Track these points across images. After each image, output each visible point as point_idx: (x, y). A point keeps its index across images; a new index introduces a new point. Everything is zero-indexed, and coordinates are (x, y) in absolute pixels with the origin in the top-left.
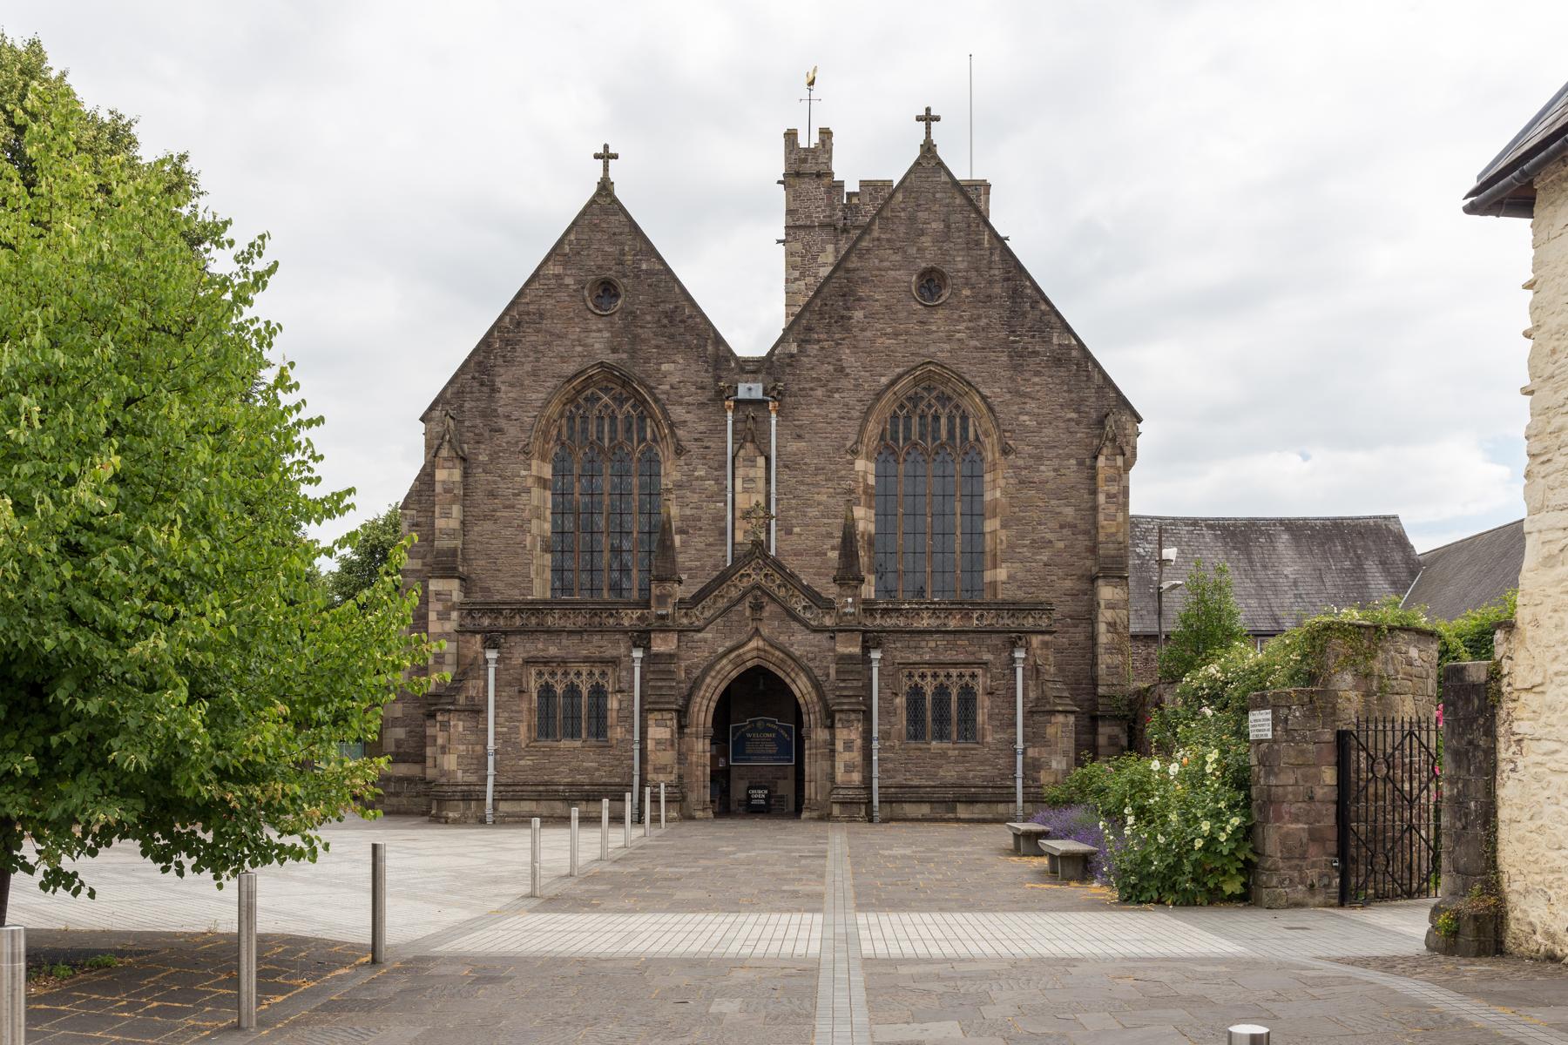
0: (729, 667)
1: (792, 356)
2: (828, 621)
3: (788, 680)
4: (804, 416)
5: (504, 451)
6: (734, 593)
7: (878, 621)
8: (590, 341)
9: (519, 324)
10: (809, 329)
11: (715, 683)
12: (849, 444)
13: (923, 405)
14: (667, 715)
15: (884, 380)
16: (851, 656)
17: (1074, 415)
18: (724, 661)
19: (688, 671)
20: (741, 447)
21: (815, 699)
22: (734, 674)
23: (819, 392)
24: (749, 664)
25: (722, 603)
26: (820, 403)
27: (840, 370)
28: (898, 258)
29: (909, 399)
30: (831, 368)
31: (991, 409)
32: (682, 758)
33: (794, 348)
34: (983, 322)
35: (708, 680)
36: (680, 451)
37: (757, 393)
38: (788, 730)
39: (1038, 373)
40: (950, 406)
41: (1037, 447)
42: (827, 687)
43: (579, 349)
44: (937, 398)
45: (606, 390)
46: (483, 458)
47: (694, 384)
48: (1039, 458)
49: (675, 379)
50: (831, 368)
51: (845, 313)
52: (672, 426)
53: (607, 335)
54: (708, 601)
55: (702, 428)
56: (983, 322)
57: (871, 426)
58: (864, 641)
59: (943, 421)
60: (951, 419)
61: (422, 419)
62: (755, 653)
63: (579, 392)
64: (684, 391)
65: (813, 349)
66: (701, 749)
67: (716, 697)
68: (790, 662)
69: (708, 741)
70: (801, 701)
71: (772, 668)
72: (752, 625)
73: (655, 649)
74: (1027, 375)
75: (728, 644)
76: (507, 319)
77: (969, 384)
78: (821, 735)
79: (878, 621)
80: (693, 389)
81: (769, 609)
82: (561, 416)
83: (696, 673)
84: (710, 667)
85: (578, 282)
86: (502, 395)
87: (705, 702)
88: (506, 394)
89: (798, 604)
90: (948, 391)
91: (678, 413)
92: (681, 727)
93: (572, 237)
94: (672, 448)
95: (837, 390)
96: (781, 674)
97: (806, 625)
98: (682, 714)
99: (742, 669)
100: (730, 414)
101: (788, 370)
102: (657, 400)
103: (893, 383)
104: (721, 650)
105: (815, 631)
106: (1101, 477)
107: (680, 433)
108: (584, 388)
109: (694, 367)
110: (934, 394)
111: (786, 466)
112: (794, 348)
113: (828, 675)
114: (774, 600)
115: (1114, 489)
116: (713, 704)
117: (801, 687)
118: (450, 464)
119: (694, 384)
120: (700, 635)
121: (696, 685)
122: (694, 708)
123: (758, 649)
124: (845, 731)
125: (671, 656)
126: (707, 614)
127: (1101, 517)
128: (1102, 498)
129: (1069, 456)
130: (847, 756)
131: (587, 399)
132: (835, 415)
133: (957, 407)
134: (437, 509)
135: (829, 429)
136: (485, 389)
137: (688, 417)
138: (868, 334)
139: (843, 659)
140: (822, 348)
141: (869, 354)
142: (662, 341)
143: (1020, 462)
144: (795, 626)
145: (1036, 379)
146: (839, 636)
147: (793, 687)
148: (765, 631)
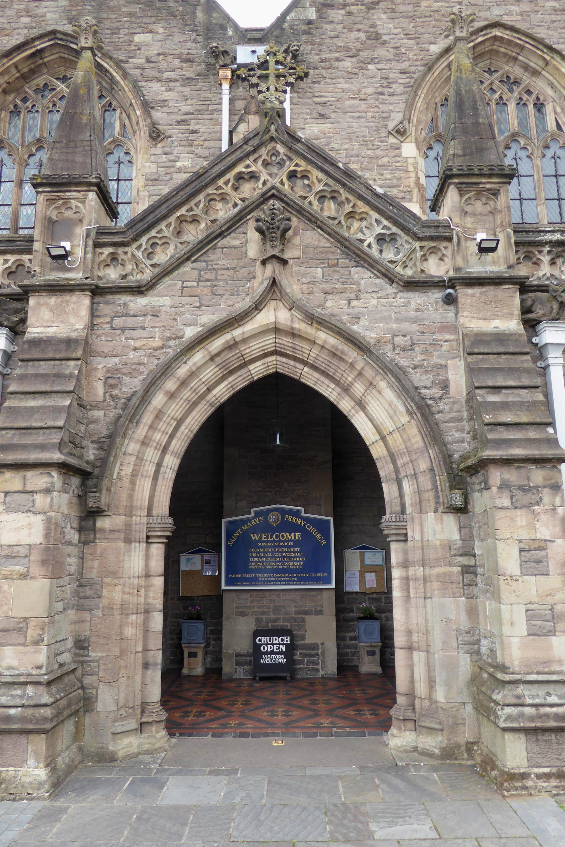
0: (210, 373)
1: (310, 22)
2: (436, 268)
3: (345, 405)
6: (223, 213)
7: (545, 269)
8: (40, 11)
11: (175, 410)
12: (391, 125)
14: (37, 480)
16: (500, 338)
18: (199, 357)
19: (112, 380)
20: (241, 120)
21: (417, 441)
22: (222, 392)
23: (348, 64)
24: (257, 370)
25: (194, 234)
26: (350, 75)
27: (377, 37)
30: (362, 35)
32: (83, 592)
33: (312, 14)
35: (158, 400)
36: (156, 136)
38: (322, 526)
42: (444, 411)
43: (26, 20)
47: (178, 56)
49: (152, 52)
50: (362, 35)
52: (146, 106)
54: (165, 229)
55: (186, 108)
57: (420, 103)
58: (526, 310)
59: (512, 107)
62: (268, 342)
63: (25, 77)
64: (163, 65)
65: (337, 15)
66: (137, 570)
67: (180, 444)
68: (352, 354)
69: (158, 551)
70: (377, 451)
71: (310, 378)
72: (262, 277)
73: (35, 329)
75: (208, 318)
77: (551, 49)
78: (436, 529)
79: (545, 269)
80: (177, 62)
81: (304, 239)
83: (132, 385)
84: (166, 370)
87: (152, 455)
89: (367, 231)
90: (516, 71)
91: (154, 90)
92: (88, 516)
94: (144, 132)
95: (372, 61)
96: (329, 391)
97: (389, 277)
98: (86, 478)
99: (239, 381)
100: (226, 87)
101: (304, 38)
102: (125, 75)
104: (190, 333)
105: (411, 285)
107: (158, 115)
109: (178, 37)
112: (312, 14)
113: (445, 386)
114: (314, 221)
116: (172, 463)
117: (378, 417)
119: (178, 56)
120: (141, 301)
121: (131, 411)
122: (122, 468)
123: (276, 330)
124: (521, 518)
125: (68, 342)
126: (163, 257)
130: (532, 586)
132: (370, 91)
133: (529, 92)
135: (363, 107)
137: (167, 95)
139: (478, 347)
140: (350, 14)
141: (413, 18)
144: (363, 277)
146: (466, 295)
147: (360, 422)
148: (293, 286)
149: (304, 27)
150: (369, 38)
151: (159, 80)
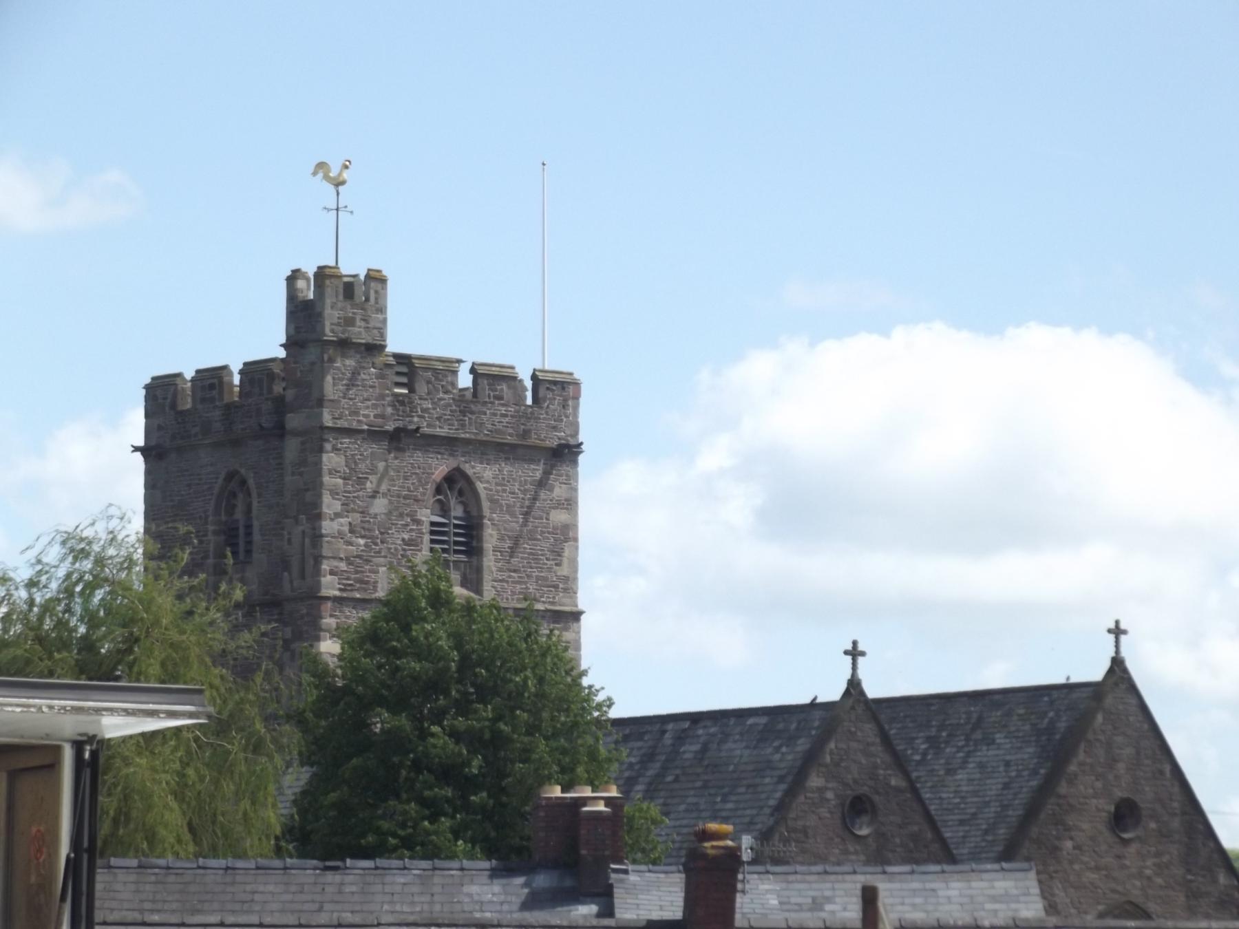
28: (1099, 785)
34: (1165, 859)
51: (1057, 843)
56: (1165, 859)
138: (1077, 867)
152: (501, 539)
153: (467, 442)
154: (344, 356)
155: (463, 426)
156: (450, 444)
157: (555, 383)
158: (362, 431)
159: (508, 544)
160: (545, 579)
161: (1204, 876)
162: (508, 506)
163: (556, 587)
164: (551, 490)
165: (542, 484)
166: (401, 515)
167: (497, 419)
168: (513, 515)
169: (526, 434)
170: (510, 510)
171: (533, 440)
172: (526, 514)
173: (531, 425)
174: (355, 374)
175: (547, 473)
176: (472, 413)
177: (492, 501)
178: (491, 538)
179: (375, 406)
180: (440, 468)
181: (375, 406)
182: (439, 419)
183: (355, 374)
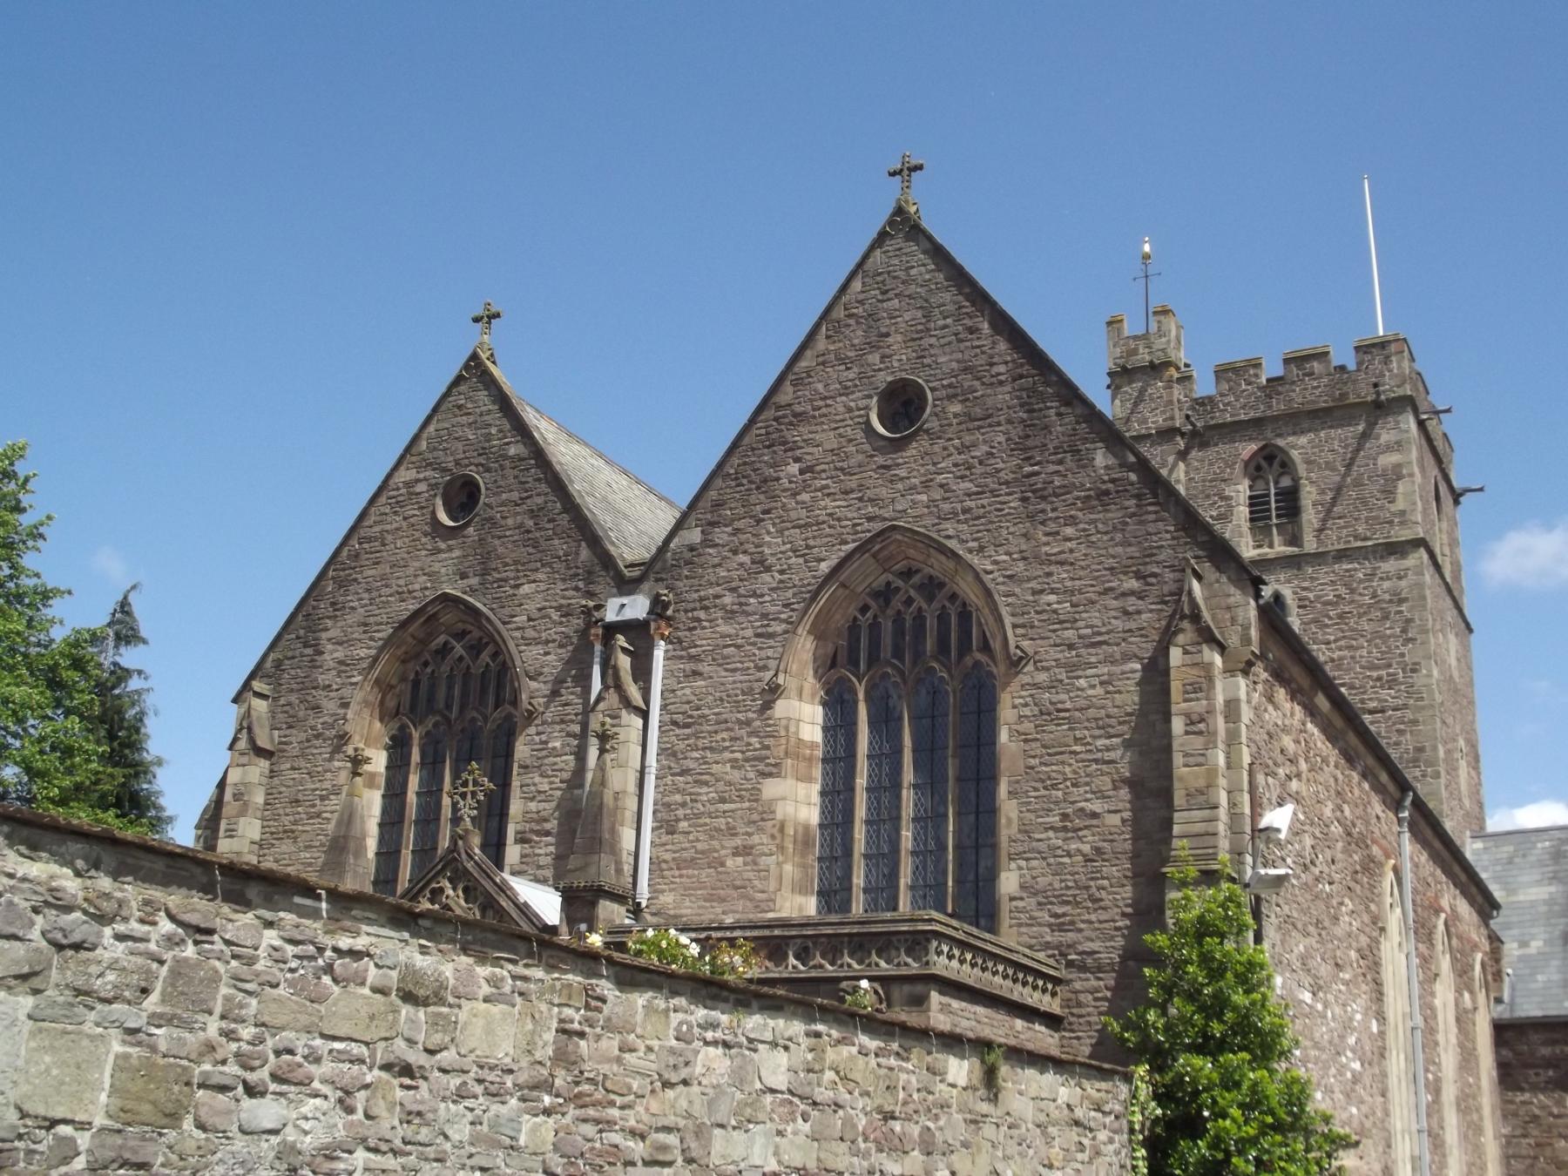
1: (692, 548)
4: (703, 640)
5: (317, 737)
9: (357, 556)
10: (718, 505)
13: (897, 603)
15: (825, 567)
17: (1134, 584)
26: (730, 615)
29: (876, 595)
31: (988, 593)
33: (694, 536)
37: (637, 607)
39: (1072, 521)
40: (941, 598)
41: (1071, 647)
44: (920, 588)
45: (460, 636)
46: (294, 749)
48: (1071, 668)
49: (531, 607)
53: (457, 553)
60: (943, 618)
61: (235, 701)
65: (721, 535)
74: (1052, 527)
76: (345, 553)
80: (555, 616)
82: (403, 679)
85: (433, 487)
86: (326, 656)
88: (332, 654)
93: (431, 428)
103: (836, 570)
106: (1176, 687)
108: (431, 636)
110: (916, 579)
111: (675, 723)
115: (1199, 706)
118: (245, 760)
119: (558, 608)
127: (1178, 759)
128: (1178, 725)
129: (1127, 658)
131: (437, 652)
134: (223, 825)
136: (309, 651)
140: (737, 531)
142: (522, 553)
143: (1042, 677)
145: (1069, 531)
149: (688, 555)
150: (753, 562)
151: (537, 641)
152: (1322, 492)
153: (1275, 419)
154: (1130, 383)
155: (1270, 407)
156: (1258, 423)
157: (1373, 345)
158: (1150, 435)
159: (1329, 496)
160: (1377, 517)
161: (1060, 462)
162: (1327, 463)
163: (1391, 522)
164: (1378, 438)
165: (1365, 436)
166: (1208, 496)
167: (1307, 393)
168: (1334, 469)
169: (1344, 396)
170: (1330, 466)
171: (1352, 399)
172: (1349, 466)
173: (1349, 388)
174: (1142, 392)
175: (1371, 425)
176: (1279, 394)
177: (1308, 462)
178: (1309, 496)
179: (1163, 412)
180: (1249, 449)
181: (1163, 412)
182: (1243, 407)
183: (1142, 392)
